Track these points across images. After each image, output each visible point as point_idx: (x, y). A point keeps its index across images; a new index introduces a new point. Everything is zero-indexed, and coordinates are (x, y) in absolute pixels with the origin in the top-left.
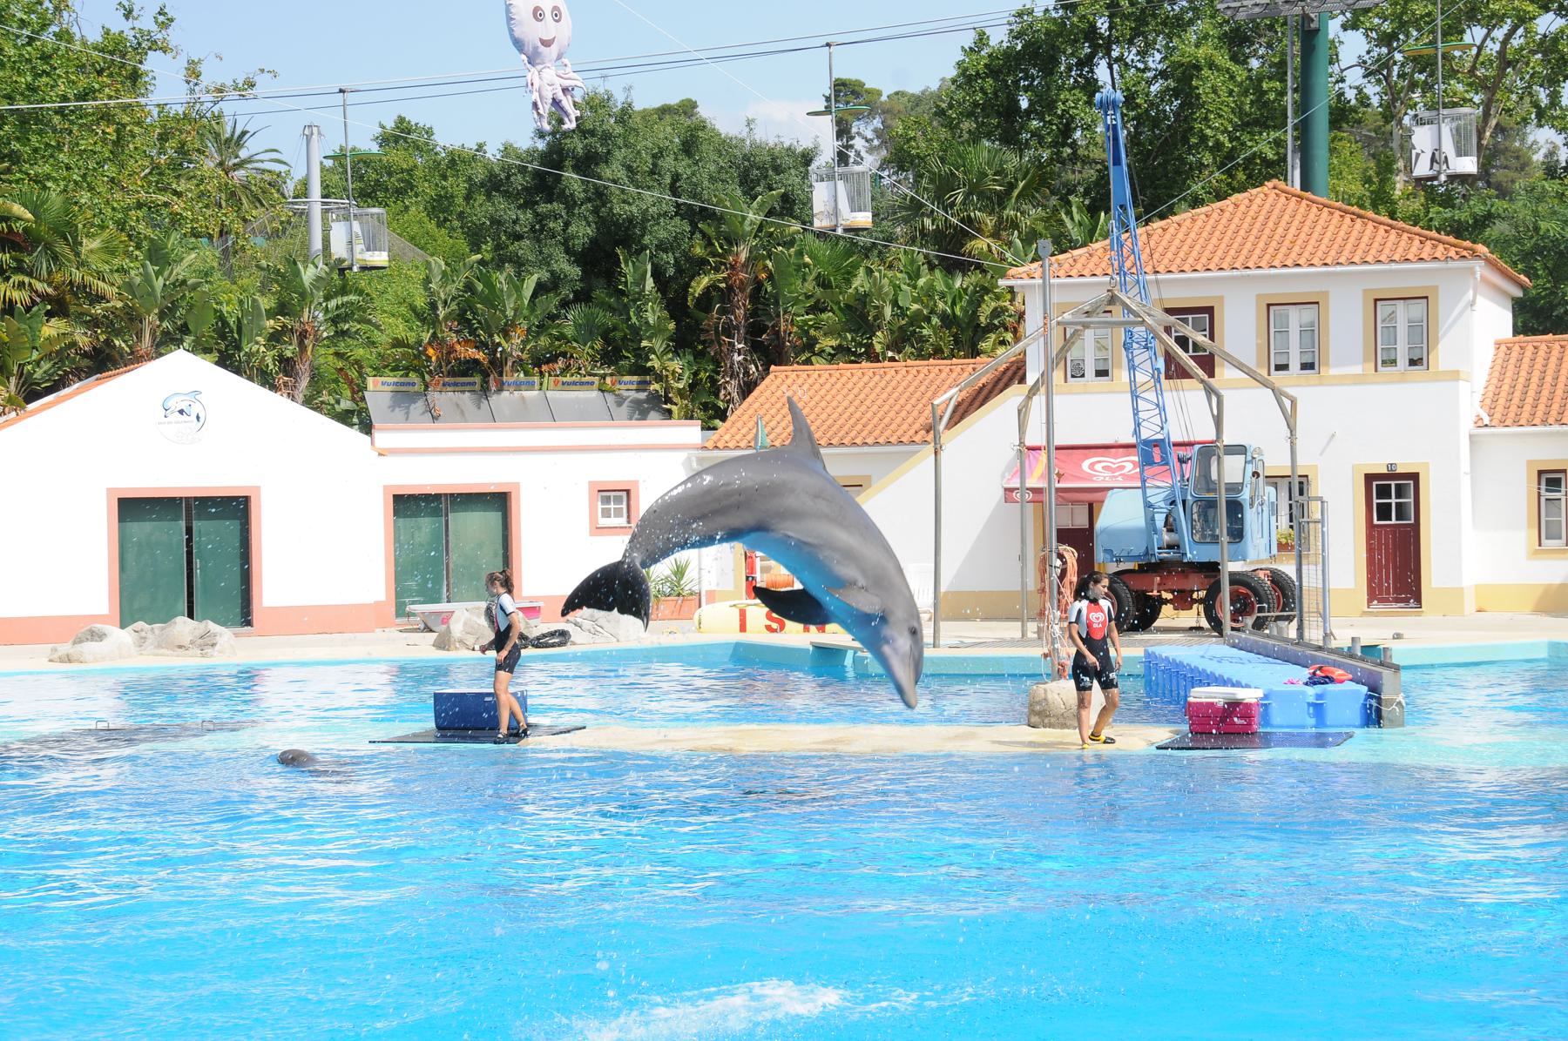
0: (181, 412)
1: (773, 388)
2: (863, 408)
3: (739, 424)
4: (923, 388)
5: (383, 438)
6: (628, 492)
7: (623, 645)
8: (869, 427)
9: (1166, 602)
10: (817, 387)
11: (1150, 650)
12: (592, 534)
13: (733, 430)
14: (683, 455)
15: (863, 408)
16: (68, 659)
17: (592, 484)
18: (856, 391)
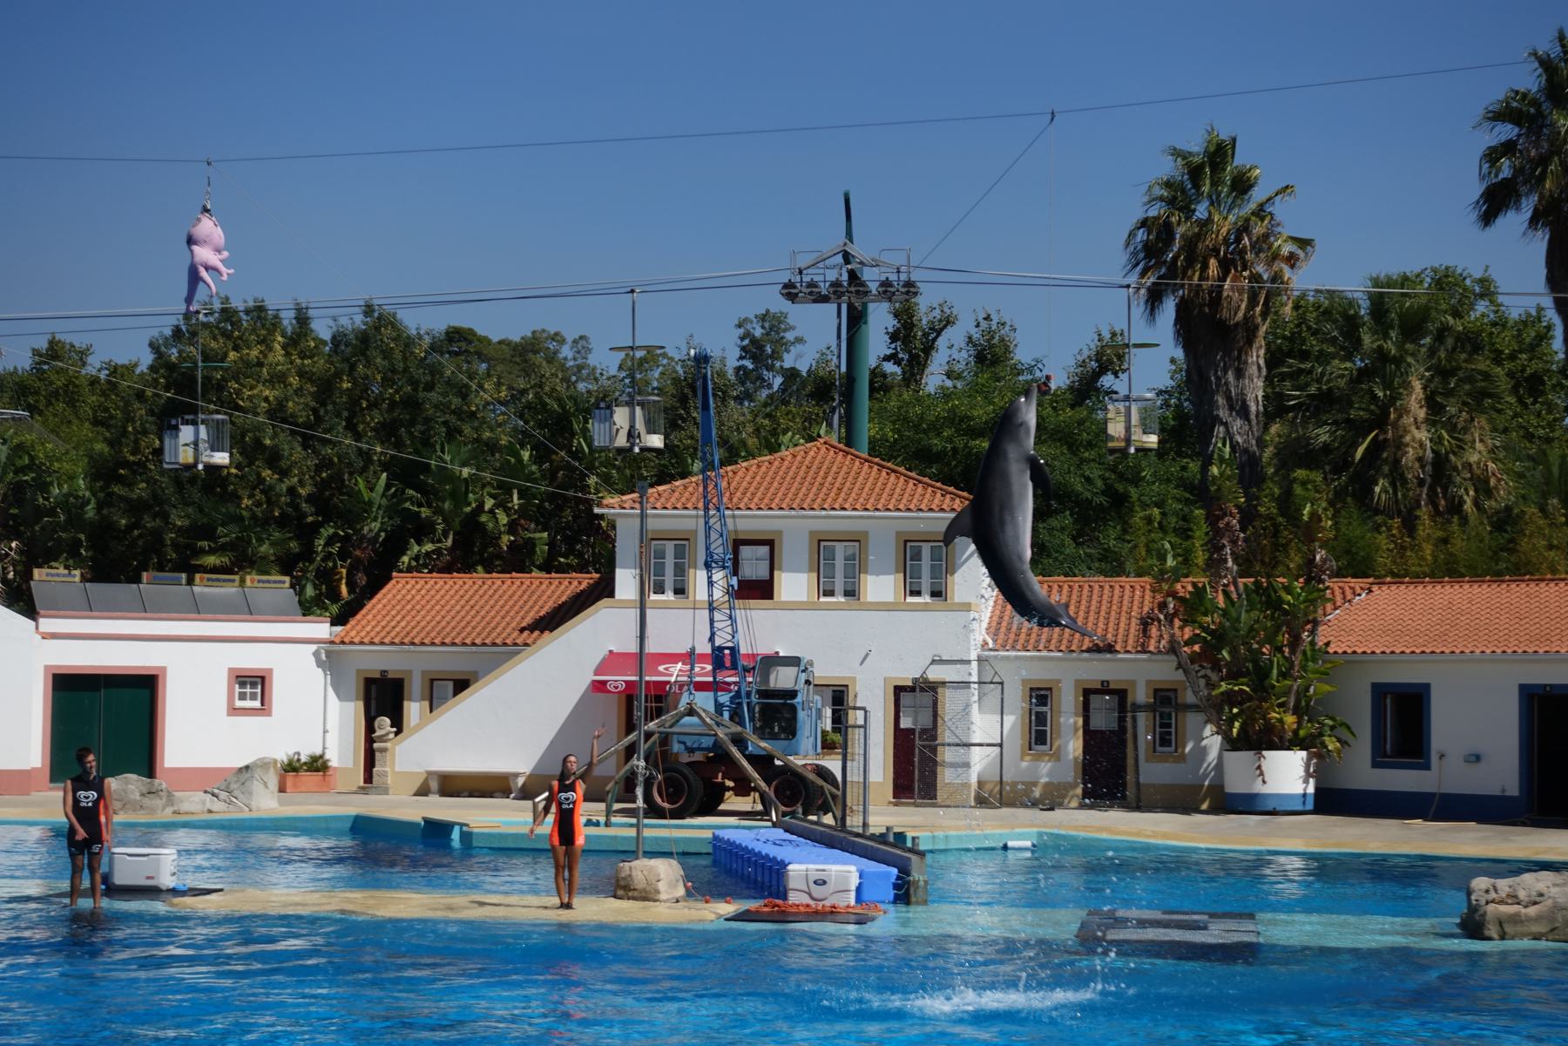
1: (394, 592)
3: (364, 622)
4: (525, 597)
5: (47, 624)
6: (263, 678)
7: (254, 815)
8: (478, 630)
9: (729, 789)
10: (432, 592)
11: (718, 832)
12: (229, 714)
13: (358, 628)
14: (314, 647)
17: (231, 670)
18: (466, 598)
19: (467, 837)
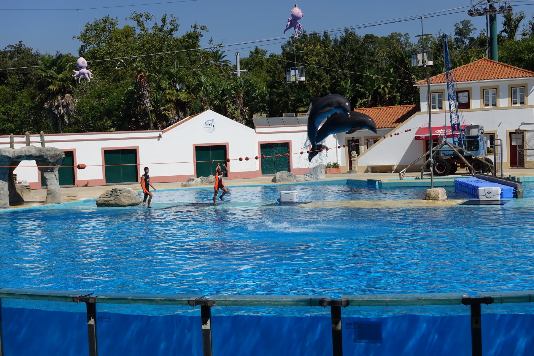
0: (210, 125)
2: (378, 119)
4: (393, 113)
5: (258, 130)
9: (458, 166)
11: (456, 179)
15: (378, 119)
16: (185, 186)
18: (376, 114)
19: (380, 184)
